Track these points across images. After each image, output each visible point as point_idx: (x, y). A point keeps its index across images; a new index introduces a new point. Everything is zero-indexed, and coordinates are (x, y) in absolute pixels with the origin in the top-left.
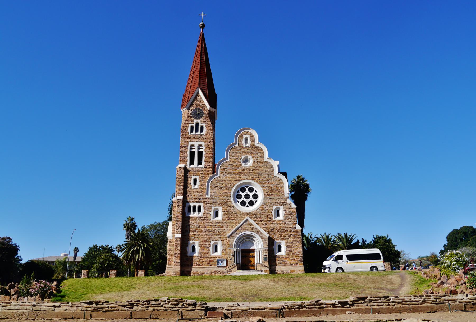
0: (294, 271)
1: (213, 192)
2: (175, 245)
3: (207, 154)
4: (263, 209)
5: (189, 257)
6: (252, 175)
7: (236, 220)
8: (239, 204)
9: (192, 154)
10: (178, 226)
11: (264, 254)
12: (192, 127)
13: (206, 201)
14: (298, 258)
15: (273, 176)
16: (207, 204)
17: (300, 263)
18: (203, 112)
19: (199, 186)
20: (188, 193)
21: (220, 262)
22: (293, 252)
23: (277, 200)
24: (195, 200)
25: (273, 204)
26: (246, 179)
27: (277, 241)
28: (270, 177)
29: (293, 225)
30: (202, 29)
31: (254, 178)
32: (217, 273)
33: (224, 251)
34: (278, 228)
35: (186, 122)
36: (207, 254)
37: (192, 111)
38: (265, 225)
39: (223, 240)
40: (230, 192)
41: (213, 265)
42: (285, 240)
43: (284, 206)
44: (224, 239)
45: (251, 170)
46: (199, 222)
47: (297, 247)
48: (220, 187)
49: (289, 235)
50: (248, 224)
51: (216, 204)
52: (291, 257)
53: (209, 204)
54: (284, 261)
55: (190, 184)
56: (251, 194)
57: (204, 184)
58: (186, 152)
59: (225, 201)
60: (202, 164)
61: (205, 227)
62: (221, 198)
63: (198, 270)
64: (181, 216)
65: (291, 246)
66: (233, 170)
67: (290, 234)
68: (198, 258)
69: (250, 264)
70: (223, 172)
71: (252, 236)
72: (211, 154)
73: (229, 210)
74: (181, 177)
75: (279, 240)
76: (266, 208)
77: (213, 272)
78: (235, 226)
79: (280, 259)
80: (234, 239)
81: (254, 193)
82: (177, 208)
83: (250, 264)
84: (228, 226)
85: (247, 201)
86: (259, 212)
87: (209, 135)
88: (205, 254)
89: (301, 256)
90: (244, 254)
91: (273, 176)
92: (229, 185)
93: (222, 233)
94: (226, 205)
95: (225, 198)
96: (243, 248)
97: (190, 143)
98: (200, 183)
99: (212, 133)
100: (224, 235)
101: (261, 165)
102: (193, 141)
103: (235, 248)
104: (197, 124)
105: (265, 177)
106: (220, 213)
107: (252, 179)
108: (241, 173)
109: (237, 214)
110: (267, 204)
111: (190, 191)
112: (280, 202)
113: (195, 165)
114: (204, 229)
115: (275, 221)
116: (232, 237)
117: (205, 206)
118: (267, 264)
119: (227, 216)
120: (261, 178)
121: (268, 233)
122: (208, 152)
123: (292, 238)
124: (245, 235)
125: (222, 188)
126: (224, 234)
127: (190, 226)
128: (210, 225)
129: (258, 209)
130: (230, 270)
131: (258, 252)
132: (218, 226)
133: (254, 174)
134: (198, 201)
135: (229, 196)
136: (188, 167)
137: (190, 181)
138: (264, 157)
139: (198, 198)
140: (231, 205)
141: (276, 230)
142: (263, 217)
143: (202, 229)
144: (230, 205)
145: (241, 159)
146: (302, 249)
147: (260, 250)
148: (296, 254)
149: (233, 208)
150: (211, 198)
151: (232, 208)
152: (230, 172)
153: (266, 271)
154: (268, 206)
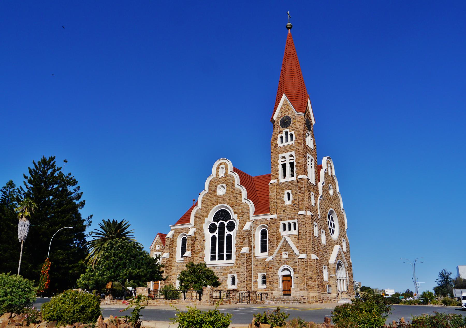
125: (324, 212)
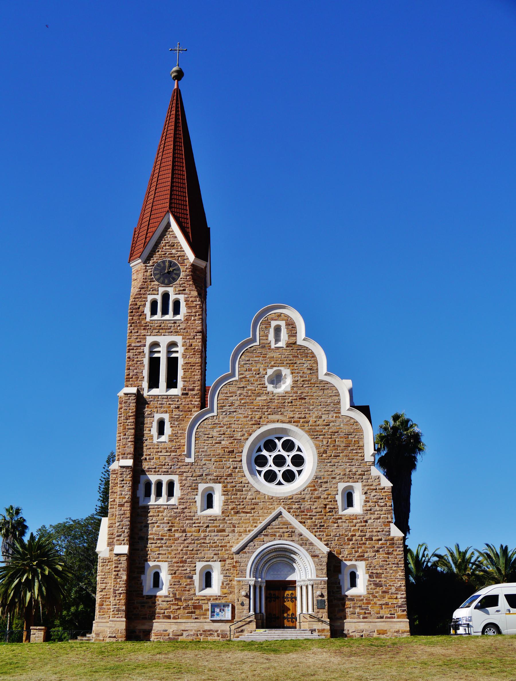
0: (386, 630)
1: (202, 450)
2: (115, 571)
3: (189, 363)
4: (315, 490)
5: (147, 599)
6: (291, 411)
7: (255, 515)
8: (261, 478)
9: (154, 363)
10: (122, 528)
11: (319, 593)
12: (154, 304)
13: (186, 470)
14: (395, 601)
15: (340, 415)
16: (188, 478)
17: (400, 613)
18: (179, 269)
19: (169, 436)
20: (145, 453)
21: (217, 610)
22: (384, 589)
23: (348, 470)
24: (162, 468)
25: (338, 477)
26: (278, 421)
27: (348, 563)
28: (331, 417)
29: (385, 526)
30: (176, 80)
31: (296, 419)
32: (211, 634)
33: (226, 585)
34: (350, 534)
35: (141, 292)
36: (187, 592)
37: (153, 266)
38: (320, 526)
39: (225, 561)
40: (240, 450)
41: (202, 617)
42: (365, 560)
43: (364, 484)
44: (227, 557)
45: (290, 400)
46: (170, 518)
47: (394, 576)
48: (218, 439)
49: (376, 549)
50: (281, 523)
51: (209, 477)
52: (379, 600)
53: (192, 478)
54: (362, 609)
55: (149, 432)
56: (288, 456)
57: (181, 431)
58: (142, 359)
59: (230, 472)
60: (176, 387)
61: (184, 531)
62: (220, 464)
63: (167, 628)
64: (128, 504)
65: (378, 575)
66: (248, 401)
67: (376, 546)
68: (168, 601)
69: (285, 615)
70: (224, 406)
71: (292, 550)
72: (197, 365)
73: (239, 490)
74: (130, 416)
75: (351, 560)
76: (324, 486)
77: (202, 632)
78: (252, 529)
79: (355, 604)
80: (249, 558)
81: (294, 453)
82: (120, 487)
83: (285, 615)
84: (236, 529)
85: (279, 471)
86: (307, 497)
87: (193, 322)
88: (184, 590)
89: (401, 597)
90: (272, 592)
91: (340, 415)
92: (238, 435)
93: (223, 544)
94: (231, 481)
95: (230, 463)
96: (270, 578)
97: (150, 340)
98: (173, 430)
99: (201, 317)
100: (227, 548)
101: (311, 389)
102: (156, 335)
103: (252, 578)
104: (166, 297)
105: (321, 417)
106: (218, 499)
107: (290, 422)
108: (266, 407)
109: (257, 501)
110: (324, 478)
111: (150, 449)
112: (355, 474)
113: (161, 390)
114: (180, 534)
115: (343, 517)
116: (245, 553)
117: (184, 482)
118: (324, 614)
119: (234, 506)
120: (312, 420)
121: (327, 545)
122: (190, 359)
123: (382, 555)
124: (275, 549)
125: (223, 442)
126: (226, 546)
127: (150, 529)
128: (195, 527)
129: (304, 491)
130: (240, 630)
131: (304, 589)
132: (213, 528)
133: (296, 410)
134: (168, 472)
135: (239, 460)
136: (146, 393)
137: (150, 426)
138: (317, 372)
139: (168, 465)
140: (243, 480)
141: (346, 538)
142: (316, 508)
143: (177, 535)
144: (241, 481)
145: (266, 377)
146: (404, 582)
147: (308, 583)
148: (392, 593)
149: (248, 486)
150: (196, 464)
151: (244, 487)
152: (239, 406)
153: (323, 630)
154: (327, 482)
